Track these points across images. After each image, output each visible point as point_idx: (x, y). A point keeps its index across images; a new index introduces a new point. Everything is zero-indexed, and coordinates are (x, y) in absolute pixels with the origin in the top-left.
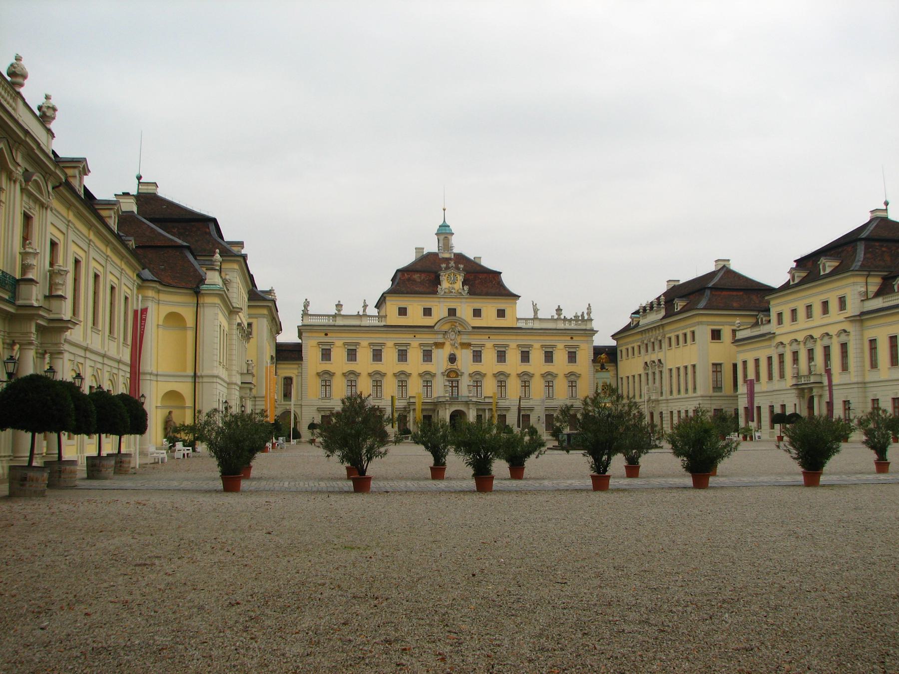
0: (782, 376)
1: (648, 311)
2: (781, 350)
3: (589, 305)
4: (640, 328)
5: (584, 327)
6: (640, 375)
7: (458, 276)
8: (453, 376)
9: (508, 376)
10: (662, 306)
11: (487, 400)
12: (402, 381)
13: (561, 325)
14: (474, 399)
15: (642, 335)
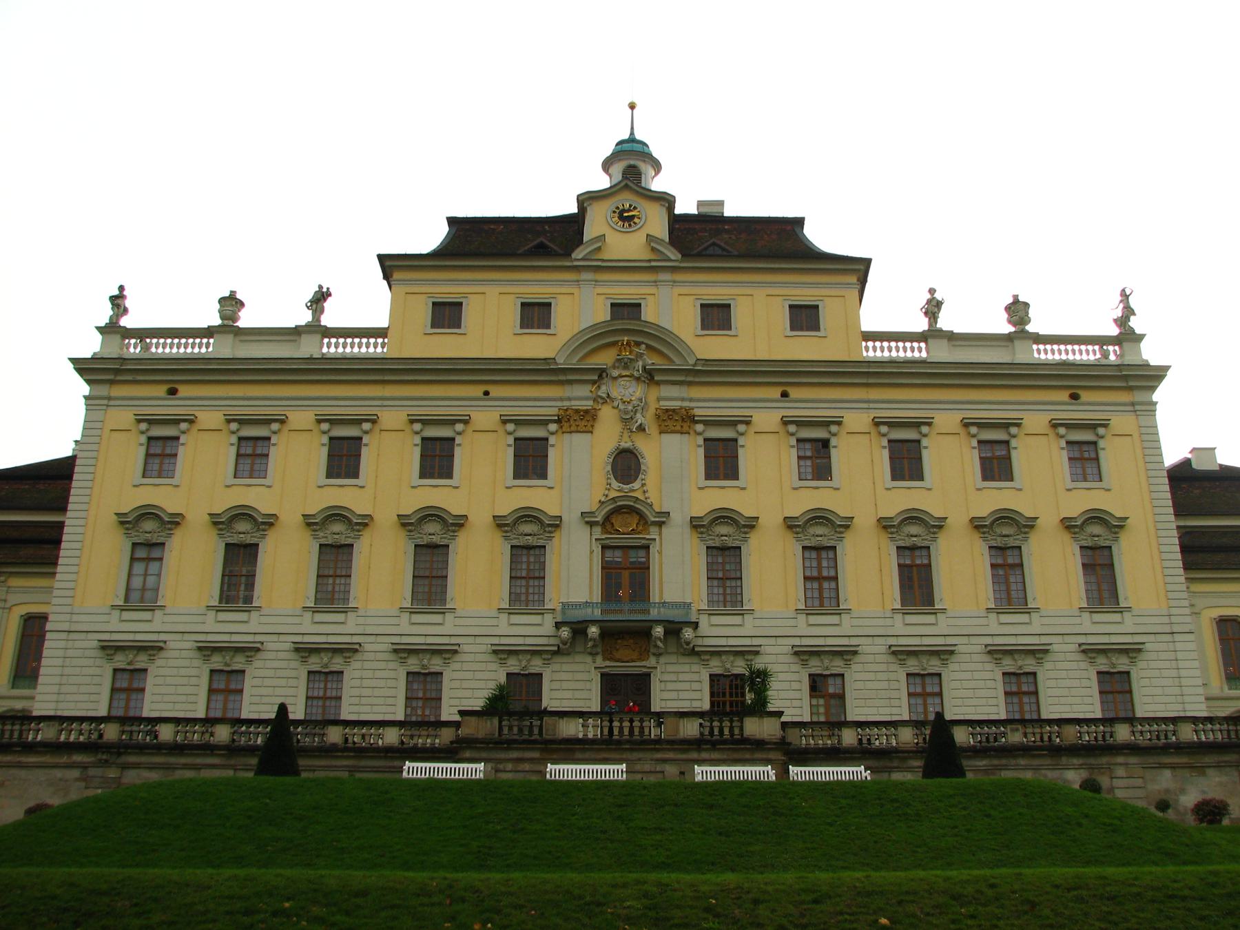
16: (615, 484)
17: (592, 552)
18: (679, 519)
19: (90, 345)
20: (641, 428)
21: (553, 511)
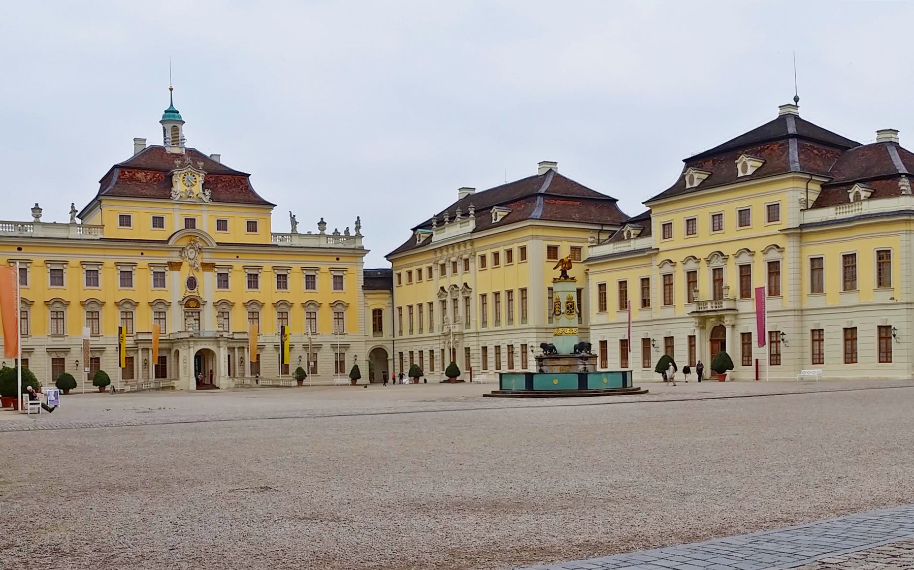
0: (668, 301)
1: (447, 223)
2: (667, 269)
3: (358, 217)
4: (433, 245)
5: (353, 246)
6: (431, 304)
7: (197, 176)
8: (192, 305)
9: (262, 305)
10: (472, 216)
11: (236, 336)
12: (126, 313)
13: (323, 243)
14: (225, 335)
15: (435, 254)
16: (189, 290)
17: (182, 314)
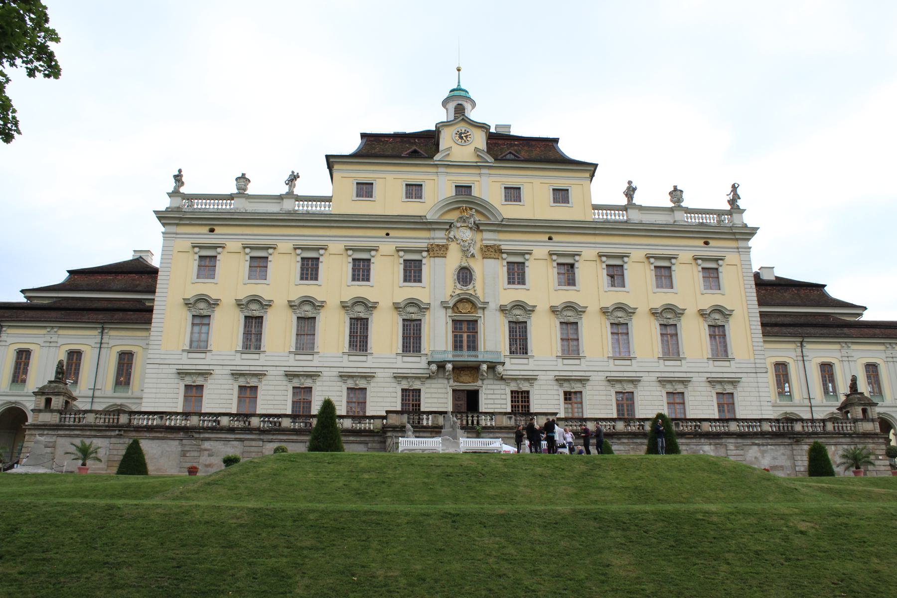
17: (447, 323)
18: (493, 306)
19: (164, 203)
20: (473, 256)
21: (426, 301)
